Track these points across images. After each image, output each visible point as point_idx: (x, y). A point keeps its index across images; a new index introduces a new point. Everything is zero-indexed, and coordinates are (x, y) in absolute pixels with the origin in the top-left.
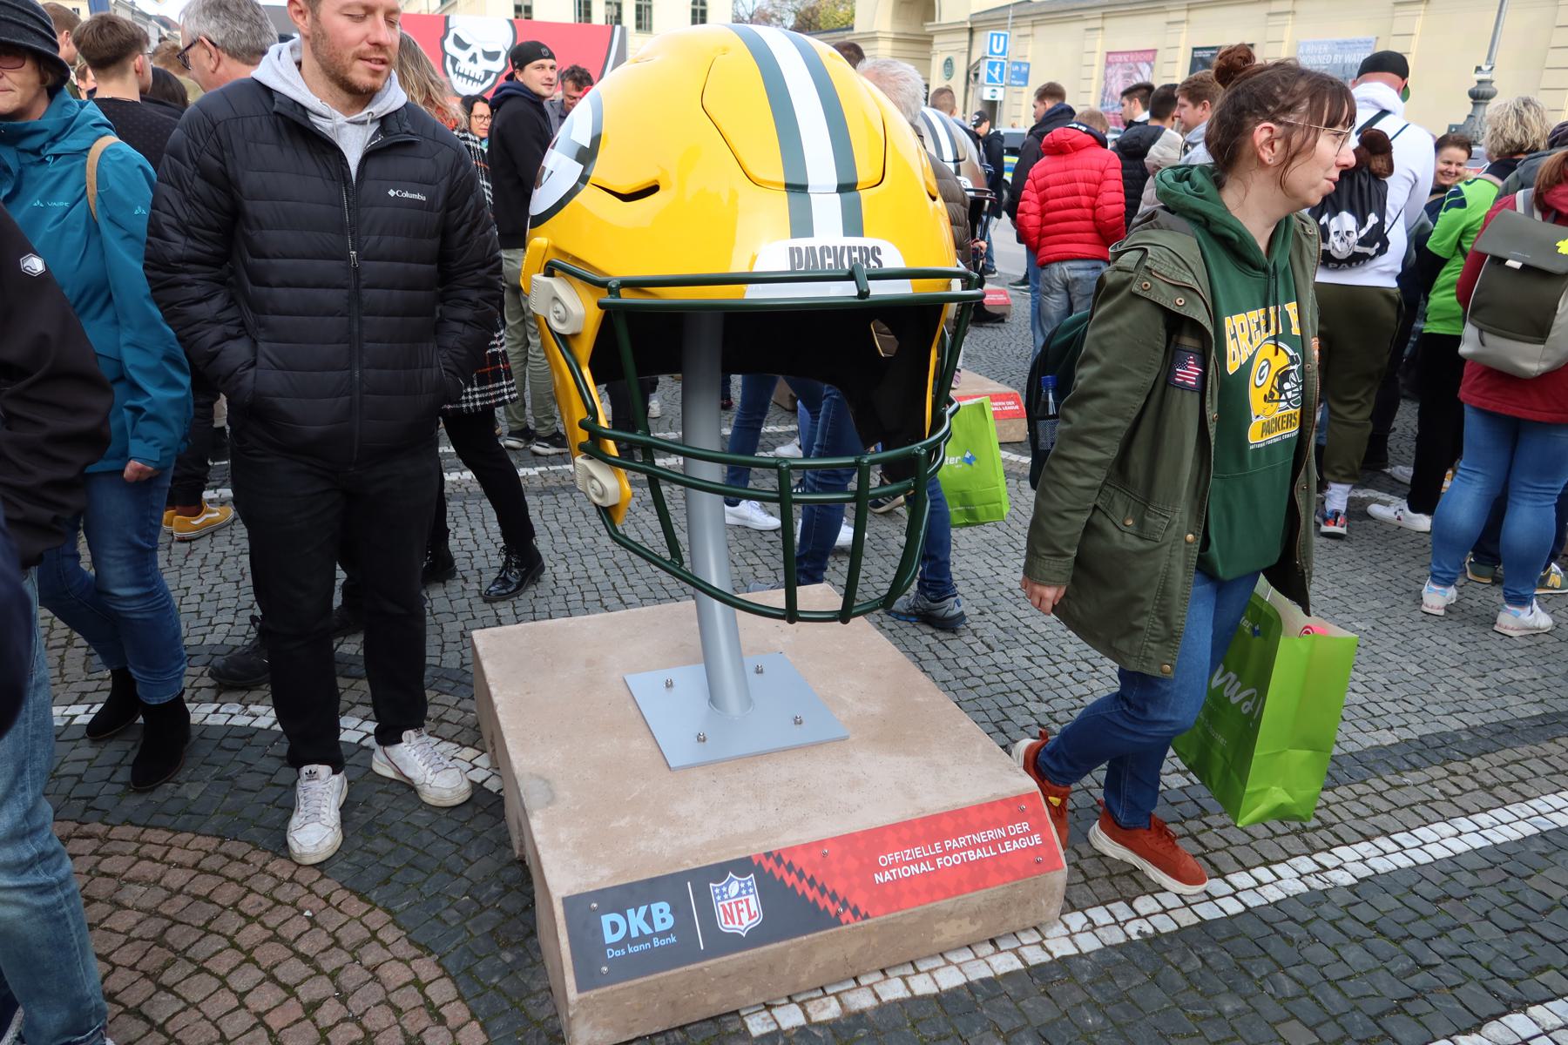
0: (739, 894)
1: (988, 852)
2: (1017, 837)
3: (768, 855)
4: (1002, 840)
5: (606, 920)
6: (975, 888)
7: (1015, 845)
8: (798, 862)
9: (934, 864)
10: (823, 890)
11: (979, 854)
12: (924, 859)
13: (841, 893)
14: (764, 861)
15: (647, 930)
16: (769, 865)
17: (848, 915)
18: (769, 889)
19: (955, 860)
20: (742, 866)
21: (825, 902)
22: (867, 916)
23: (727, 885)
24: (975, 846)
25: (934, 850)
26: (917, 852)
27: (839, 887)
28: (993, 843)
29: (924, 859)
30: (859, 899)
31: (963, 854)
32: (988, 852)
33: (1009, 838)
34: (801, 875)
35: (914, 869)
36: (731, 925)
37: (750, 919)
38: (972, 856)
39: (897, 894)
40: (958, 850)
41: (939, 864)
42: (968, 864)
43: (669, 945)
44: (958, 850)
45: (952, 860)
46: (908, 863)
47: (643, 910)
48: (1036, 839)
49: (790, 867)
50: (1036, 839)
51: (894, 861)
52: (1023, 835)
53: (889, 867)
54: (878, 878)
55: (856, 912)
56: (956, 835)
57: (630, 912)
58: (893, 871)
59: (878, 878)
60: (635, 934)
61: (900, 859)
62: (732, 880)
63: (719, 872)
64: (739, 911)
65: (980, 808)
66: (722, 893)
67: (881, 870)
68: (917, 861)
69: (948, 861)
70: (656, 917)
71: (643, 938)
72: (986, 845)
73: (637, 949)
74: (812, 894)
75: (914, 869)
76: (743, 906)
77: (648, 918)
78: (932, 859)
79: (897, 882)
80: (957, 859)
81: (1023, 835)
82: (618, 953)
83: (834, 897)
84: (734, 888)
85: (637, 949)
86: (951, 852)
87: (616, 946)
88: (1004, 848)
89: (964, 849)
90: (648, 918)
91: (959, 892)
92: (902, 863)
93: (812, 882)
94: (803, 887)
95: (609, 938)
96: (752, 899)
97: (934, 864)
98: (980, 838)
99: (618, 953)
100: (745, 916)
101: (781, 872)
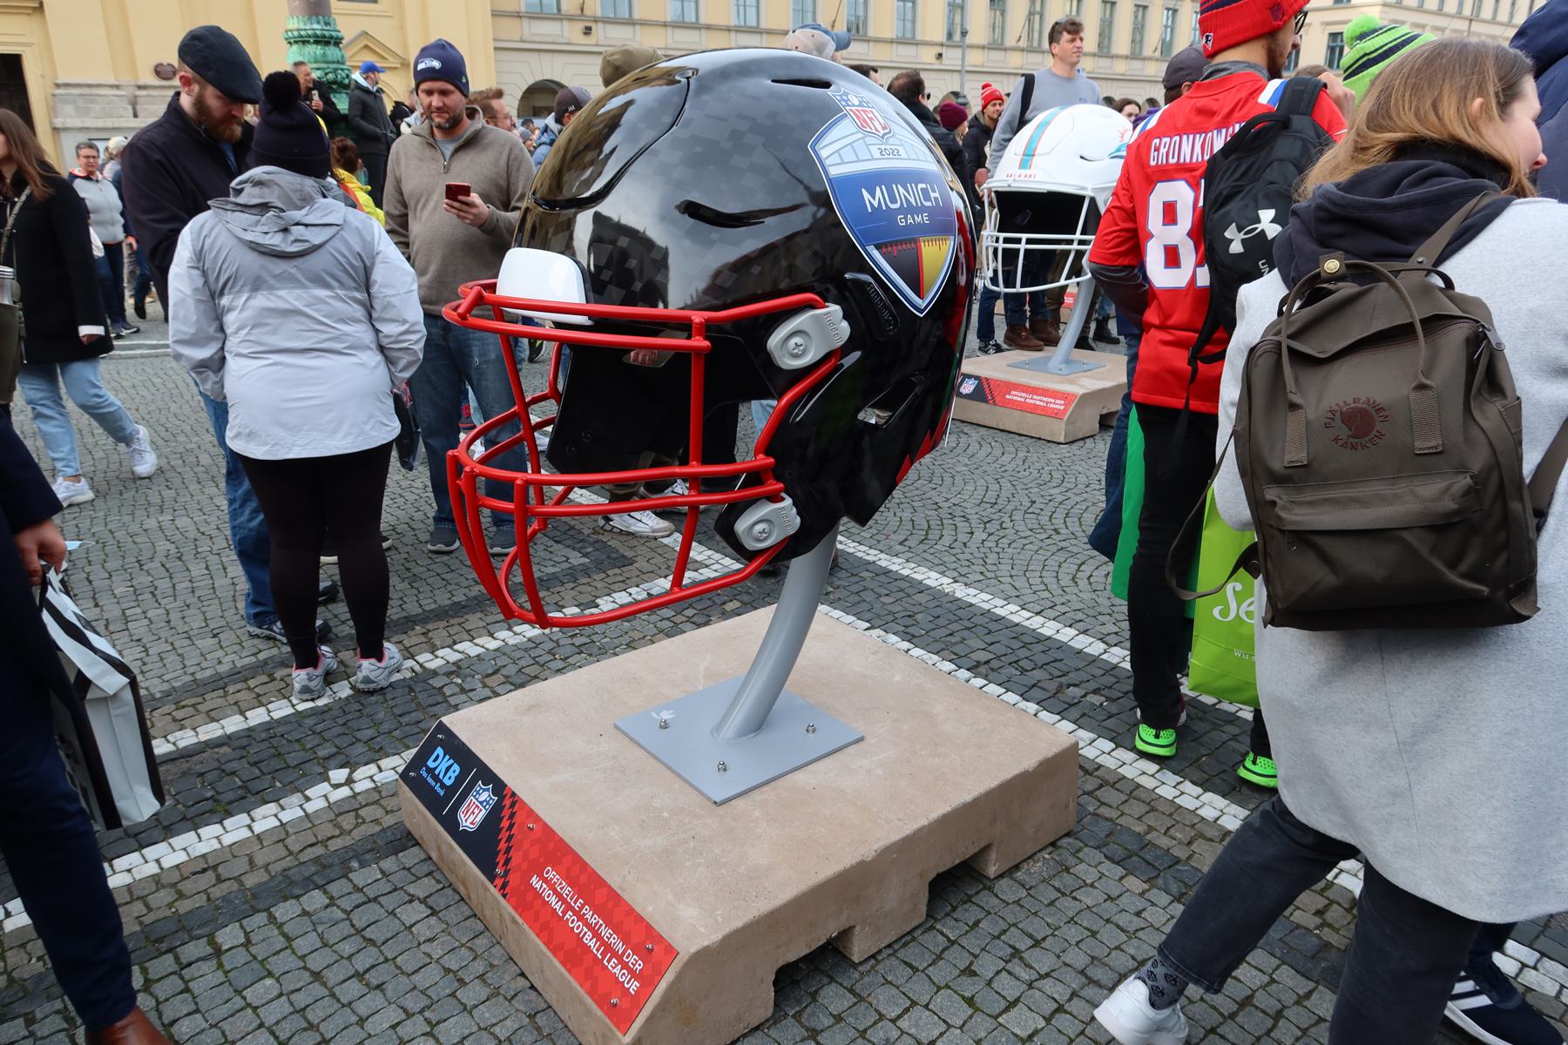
0: (481, 803)
1: (598, 950)
2: (625, 966)
3: (514, 794)
4: (615, 954)
5: (440, 751)
6: (564, 964)
8: (518, 819)
9: (564, 913)
11: (592, 944)
12: (564, 901)
13: (513, 863)
14: (508, 796)
15: (441, 777)
16: (507, 802)
17: (499, 882)
19: (576, 925)
20: (499, 787)
21: (501, 859)
22: (504, 896)
23: (484, 790)
24: (597, 935)
25: (575, 903)
26: (567, 891)
27: (516, 857)
28: (608, 949)
29: (564, 901)
30: (514, 879)
31: (585, 929)
32: (598, 950)
33: (620, 961)
34: (511, 827)
35: (553, 900)
36: (462, 816)
37: (472, 823)
39: (529, 904)
41: (567, 916)
43: (438, 794)
45: (575, 924)
46: (556, 892)
47: (451, 761)
48: (633, 986)
49: (512, 816)
50: (633, 986)
51: (552, 879)
52: (631, 972)
53: (546, 881)
54: (535, 881)
56: (596, 911)
57: (447, 757)
58: (544, 886)
59: (534, 880)
60: (437, 772)
61: (555, 883)
63: (487, 776)
64: (473, 813)
65: (631, 911)
66: (478, 793)
67: (541, 876)
69: (572, 922)
71: (436, 778)
72: (603, 943)
73: (430, 780)
74: (502, 846)
75: (553, 900)
76: (476, 811)
77: (448, 769)
78: (569, 907)
79: (538, 895)
81: (631, 972)
82: (425, 774)
83: (507, 861)
85: (430, 780)
86: (581, 918)
88: (609, 961)
90: (448, 769)
91: (554, 952)
92: (552, 887)
93: (509, 839)
94: (504, 835)
95: (431, 764)
97: (564, 913)
98: (606, 932)
99: (425, 774)
100: (472, 817)
101: (506, 813)
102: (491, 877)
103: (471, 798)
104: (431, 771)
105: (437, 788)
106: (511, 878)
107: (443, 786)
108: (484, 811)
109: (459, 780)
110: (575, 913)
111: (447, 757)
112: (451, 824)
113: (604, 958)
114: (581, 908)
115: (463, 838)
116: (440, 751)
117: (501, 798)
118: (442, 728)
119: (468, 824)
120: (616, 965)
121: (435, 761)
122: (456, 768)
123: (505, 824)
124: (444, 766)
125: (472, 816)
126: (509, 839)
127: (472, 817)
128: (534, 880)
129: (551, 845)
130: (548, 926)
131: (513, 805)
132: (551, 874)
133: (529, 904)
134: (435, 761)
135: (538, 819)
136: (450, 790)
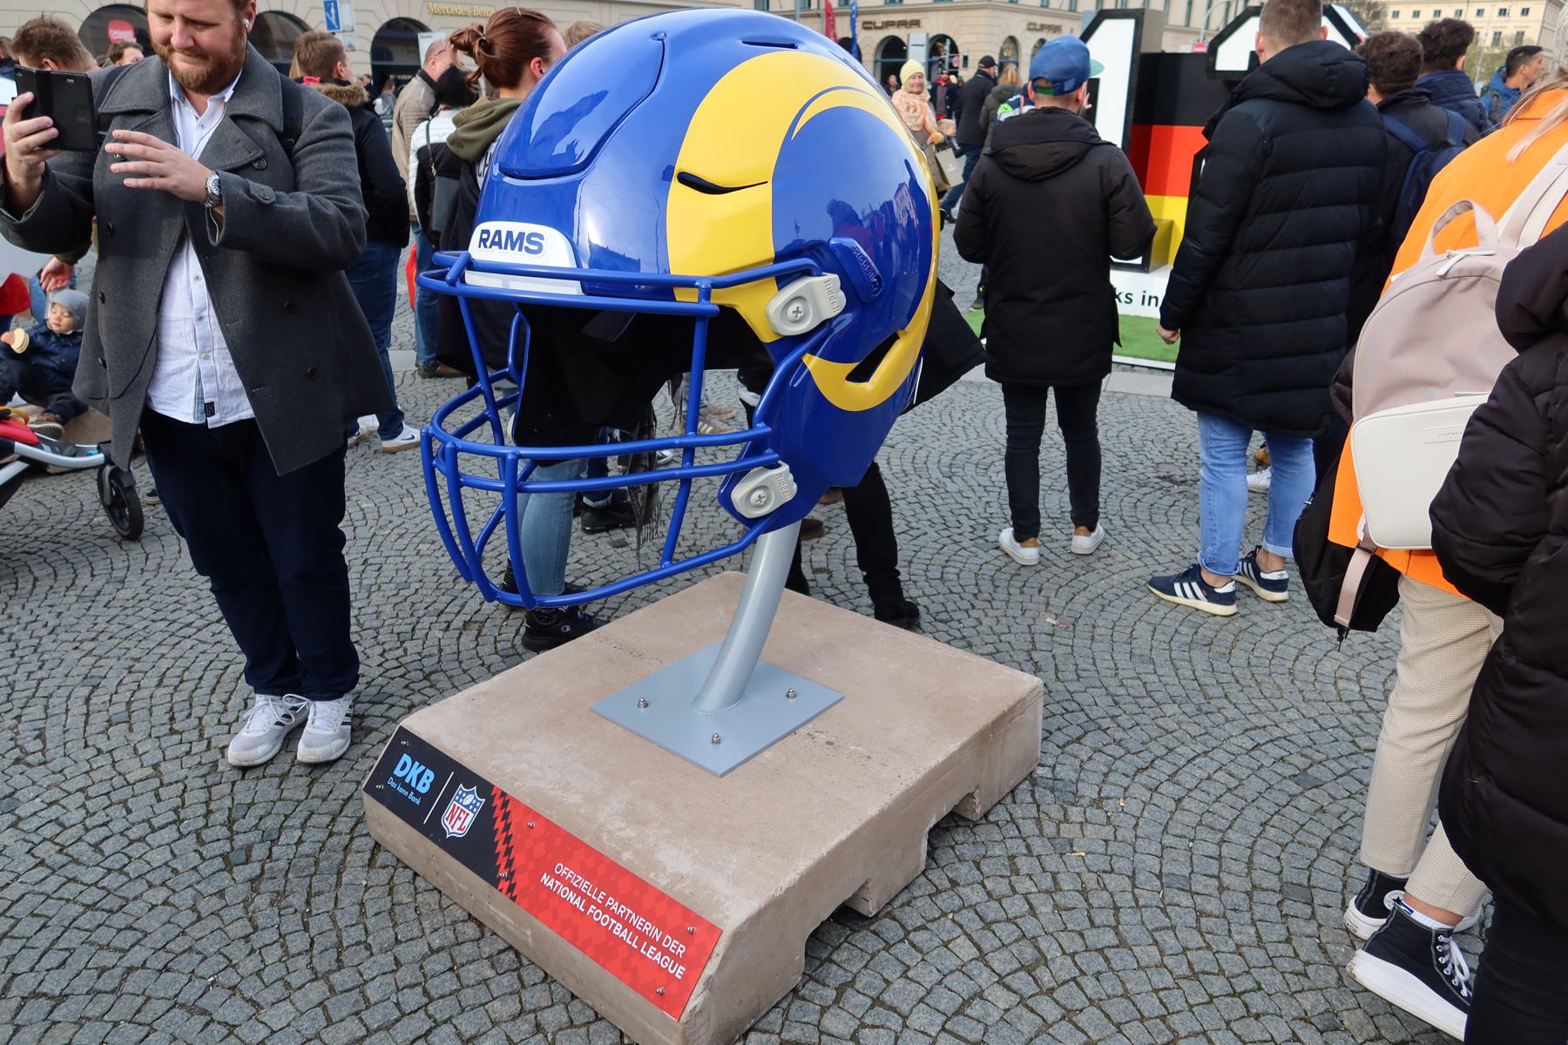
0: (467, 807)
1: (632, 940)
2: (665, 952)
3: (504, 794)
4: (652, 942)
5: (406, 758)
6: (595, 958)
7: (657, 958)
8: (514, 817)
9: (587, 907)
10: (508, 851)
11: (624, 935)
12: (584, 896)
13: (516, 865)
15: (413, 785)
16: (498, 802)
17: (504, 885)
18: (484, 822)
19: (603, 919)
20: (485, 788)
21: (502, 861)
22: (513, 899)
23: (468, 793)
24: (627, 925)
25: (597, 896)
26: (585, 885)
27: (519, 858)
28: (643, 937)
29: (584, 896)
30: (521, 881)
31: (613, 921)
32: (632, 940)
34: (507, 828)
35: (571, 896)
37: (460, 829)
38: (618, 930)
39: (544, 905)
40: (613, 915)
42: (609, 933)
43: (414, 804)
44: (613, 915)
45: (601, 917)
46: (572, 888)
47: (422, 768)
48: (679, 971)
49: (506, 816)
50: (679, 971)
52: (673, 956)
53: (558, 878)
54: (545, 879)
55: (511, 889)
56: (622, 901)
57: (417, 764)
58: (558, 883)
59: (545, 878)
60: (407, 780)
62: (472, 792)
63: (467, 777)
64: (459, 818)
66: (461, 797)
67: (552, 874)
68: (578, 892)
69: (598, 915)
70: (423, 779)
71: (408, 787)
72: (637, 932)
73: (401, 790)
74: (501, 848)
75: (571, 896)
76: (463, 816)
77: (420, 776)
78: (590, 902)
79: (552, 894)
80: (605, 920)
81: (673, 956)
83: (510, 864)
84: (469, 799)
85: (401, 790)
86: (606, 910)
87: (396, 779)
88: (646, 950)
89: (617, 918)
90: (420, 776)
91: (583, 948)
92: (568, 883)
93: (508, 839)
94: (500, 837)
95: (398, 772)
96: (471, 815)
97: (587, 907)
98: (637, 921)
99: (393, 785)
100: (459, 823)
101: (498, 813)
102: (494, 881)
103: (453, 803)
104: (401, 781)
105: (411, 796)
106: (517, 878)
107: (417, 794)
108: (471, 815)
109: (435, 786)
110: (598, 906)
111: (417, 764)
112: (434, 831)
113: (640, 947)
114: (604, 901)
115: (454, 847)
116: (406, 758)
117: (490, 800)
118: (403, 733)
119: (455, 830)
120: (656, 953)
121: (403, 768)
122: (430, 774)
123: (499, 825)
124: (415, 775)
125: (459, 818)
126: (508, 839)
127: (459, 823)
128: (545, 878)
129: (558, 842)
130: (571, 924)
131: (505, 805)
132: (563, 870)
133: (544, 905)
134: (403, 768)
135: (536, 816)
136: (428, 798)
